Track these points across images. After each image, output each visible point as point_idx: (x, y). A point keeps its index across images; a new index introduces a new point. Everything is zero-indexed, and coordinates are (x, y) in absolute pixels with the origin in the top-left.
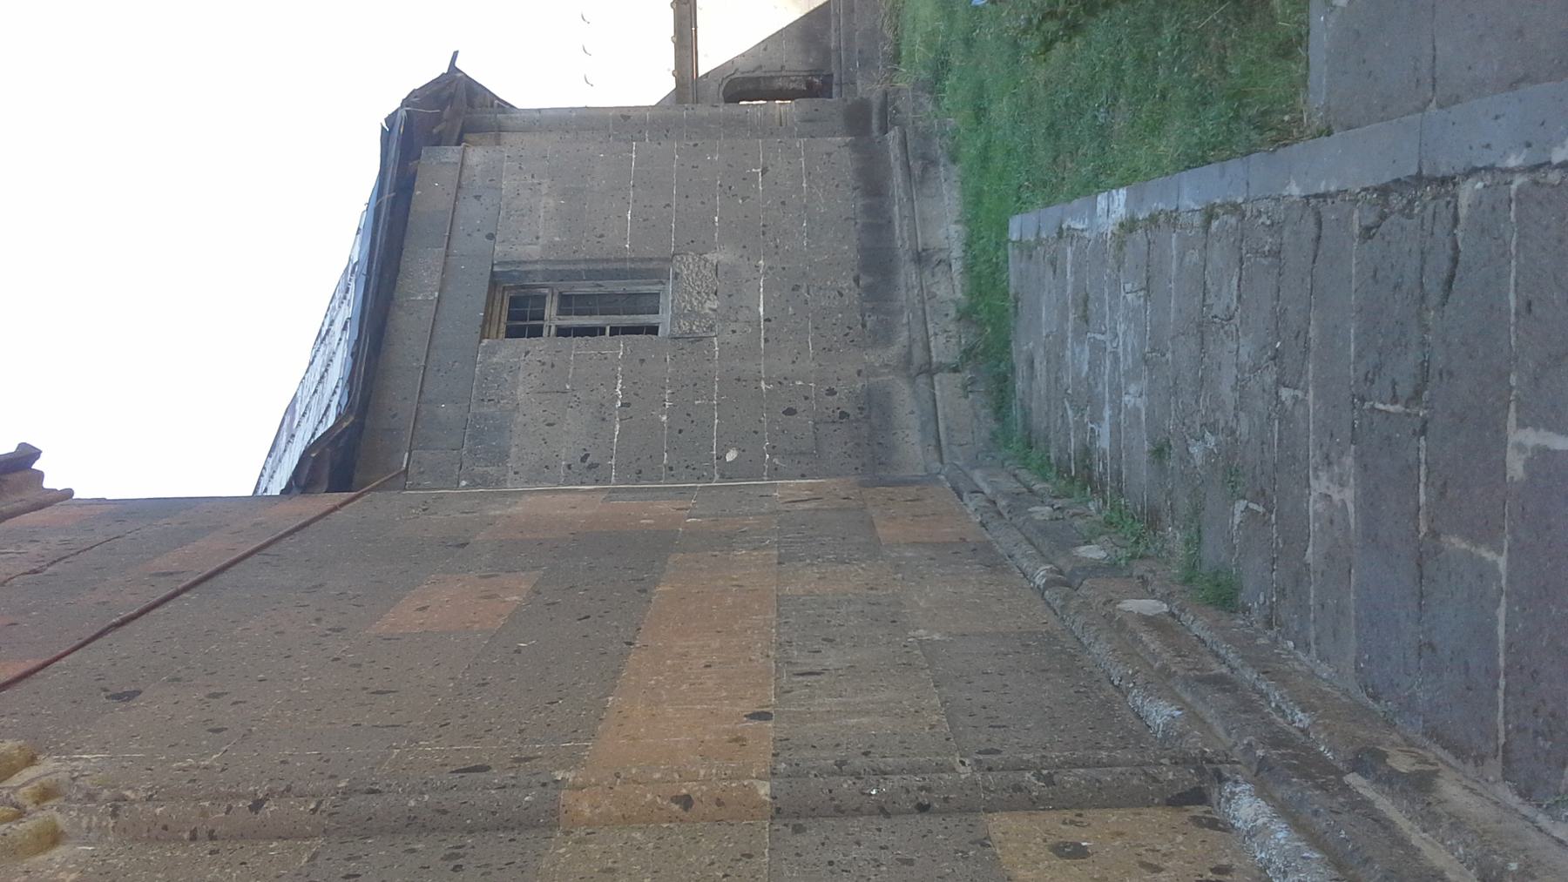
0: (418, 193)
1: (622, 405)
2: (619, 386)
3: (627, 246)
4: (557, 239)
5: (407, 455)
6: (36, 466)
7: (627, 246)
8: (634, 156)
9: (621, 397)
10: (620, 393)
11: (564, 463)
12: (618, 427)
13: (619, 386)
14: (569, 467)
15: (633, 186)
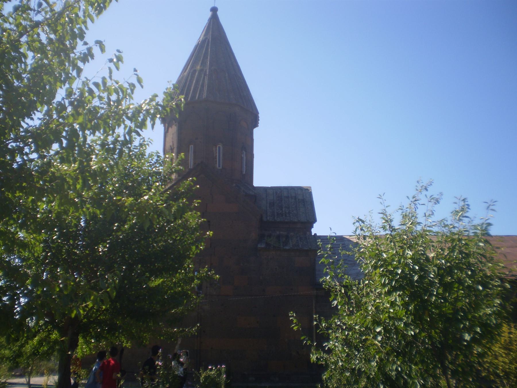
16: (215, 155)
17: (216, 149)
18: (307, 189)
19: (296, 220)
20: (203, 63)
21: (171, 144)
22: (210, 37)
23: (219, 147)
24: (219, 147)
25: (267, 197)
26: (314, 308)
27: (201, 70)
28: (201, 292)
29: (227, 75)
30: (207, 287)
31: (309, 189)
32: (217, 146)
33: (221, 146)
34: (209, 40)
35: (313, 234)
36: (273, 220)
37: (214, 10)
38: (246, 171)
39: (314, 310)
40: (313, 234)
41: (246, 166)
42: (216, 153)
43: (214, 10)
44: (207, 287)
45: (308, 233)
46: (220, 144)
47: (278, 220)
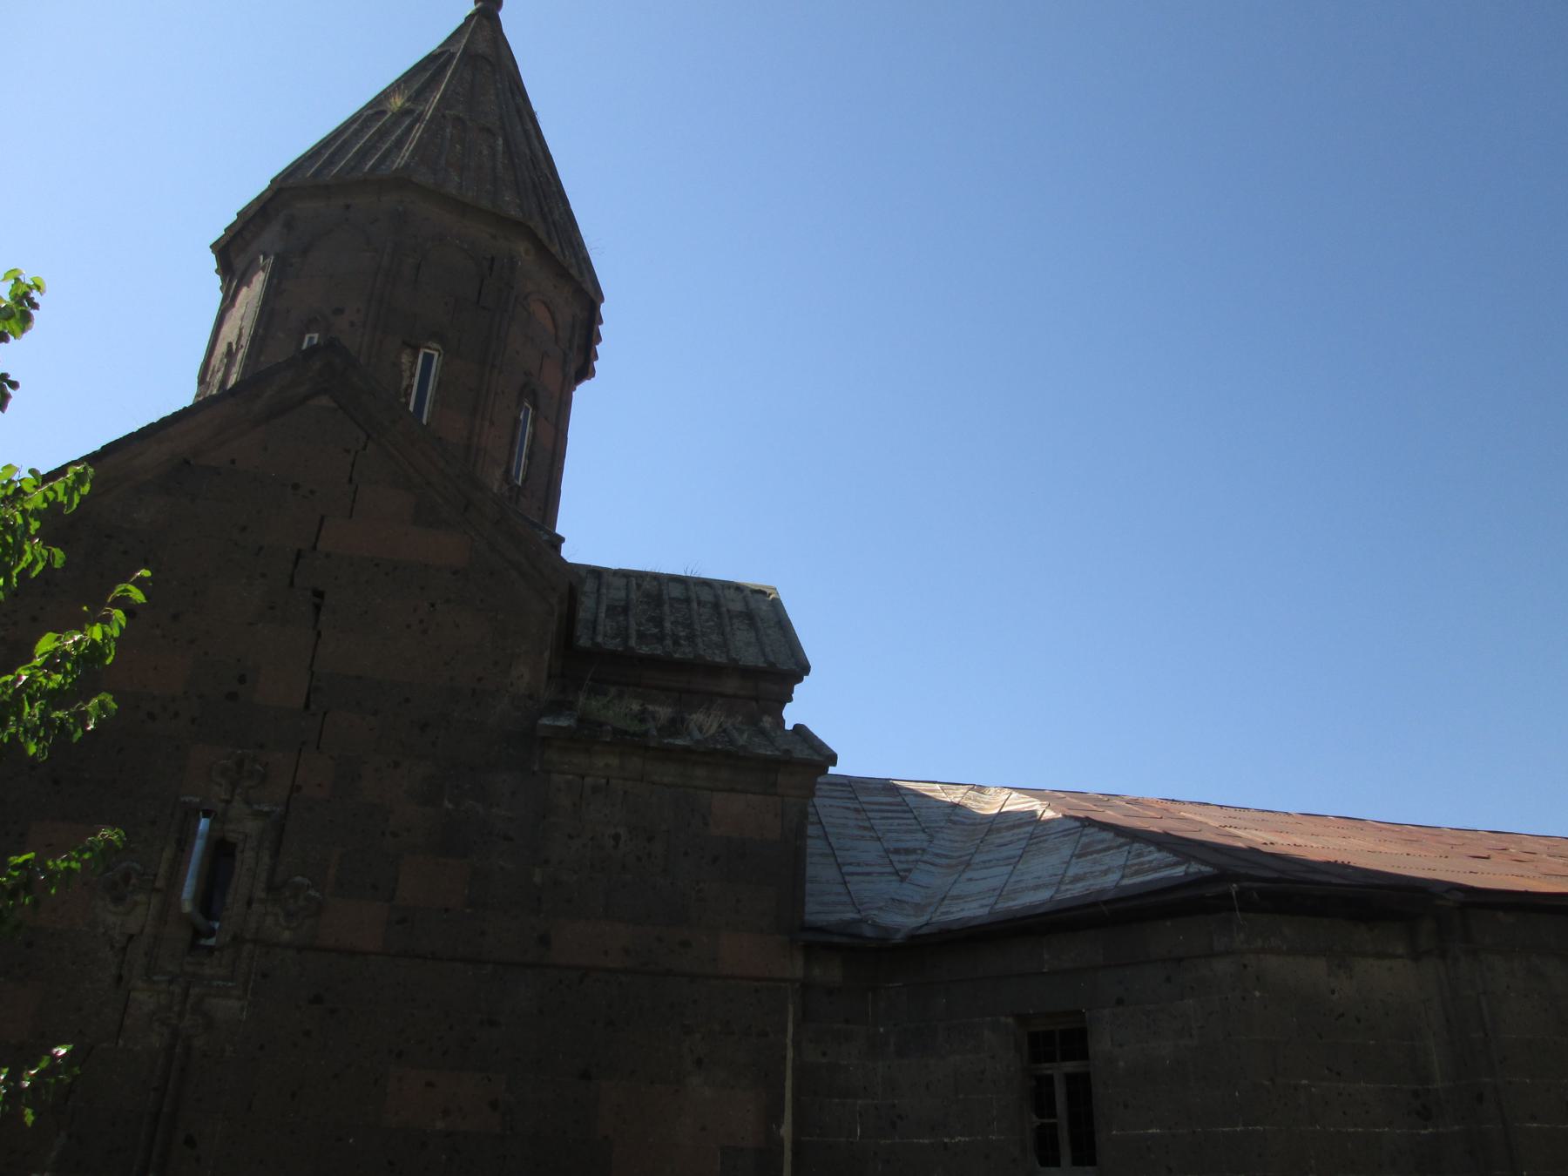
0: (1168, 923)
1: (946, 1143)
2: (963, 1139)
3: (1114, 1132)
4: (1121, 1064)
5: (900, 984)
7: (1114, 1132)
8: (1238, 1129)
9: (953, 1141)
10: (957, 1140)
11: (896, 1102)
12: (926, 1141)
13: (963, 1139)
14: (894, 1106)
15: (1194, 1132)
16: (405, 383)
17: (414, 363)
19: (720, 659)
20: (419, 96)
21: (233, 338)
22: (458, 49)
23: (428, 359)
24: (428, 359)
25: (598, 590)
26: (789, 1042)
27: (404, 112)
28: (217, 925)
29: (500, 141)
30: (249, 903)
31: (768, 591)
33: (436, 354)
34: (452, 55)
35: (789, 726)
36: (620, 649)
38: (524, 481)
39: (790, 1054)
40: (789, 726)
41: (530, 457)
42: (413, 375)
44: (249, 903)
45: (767, 721)
46: (435, 345)
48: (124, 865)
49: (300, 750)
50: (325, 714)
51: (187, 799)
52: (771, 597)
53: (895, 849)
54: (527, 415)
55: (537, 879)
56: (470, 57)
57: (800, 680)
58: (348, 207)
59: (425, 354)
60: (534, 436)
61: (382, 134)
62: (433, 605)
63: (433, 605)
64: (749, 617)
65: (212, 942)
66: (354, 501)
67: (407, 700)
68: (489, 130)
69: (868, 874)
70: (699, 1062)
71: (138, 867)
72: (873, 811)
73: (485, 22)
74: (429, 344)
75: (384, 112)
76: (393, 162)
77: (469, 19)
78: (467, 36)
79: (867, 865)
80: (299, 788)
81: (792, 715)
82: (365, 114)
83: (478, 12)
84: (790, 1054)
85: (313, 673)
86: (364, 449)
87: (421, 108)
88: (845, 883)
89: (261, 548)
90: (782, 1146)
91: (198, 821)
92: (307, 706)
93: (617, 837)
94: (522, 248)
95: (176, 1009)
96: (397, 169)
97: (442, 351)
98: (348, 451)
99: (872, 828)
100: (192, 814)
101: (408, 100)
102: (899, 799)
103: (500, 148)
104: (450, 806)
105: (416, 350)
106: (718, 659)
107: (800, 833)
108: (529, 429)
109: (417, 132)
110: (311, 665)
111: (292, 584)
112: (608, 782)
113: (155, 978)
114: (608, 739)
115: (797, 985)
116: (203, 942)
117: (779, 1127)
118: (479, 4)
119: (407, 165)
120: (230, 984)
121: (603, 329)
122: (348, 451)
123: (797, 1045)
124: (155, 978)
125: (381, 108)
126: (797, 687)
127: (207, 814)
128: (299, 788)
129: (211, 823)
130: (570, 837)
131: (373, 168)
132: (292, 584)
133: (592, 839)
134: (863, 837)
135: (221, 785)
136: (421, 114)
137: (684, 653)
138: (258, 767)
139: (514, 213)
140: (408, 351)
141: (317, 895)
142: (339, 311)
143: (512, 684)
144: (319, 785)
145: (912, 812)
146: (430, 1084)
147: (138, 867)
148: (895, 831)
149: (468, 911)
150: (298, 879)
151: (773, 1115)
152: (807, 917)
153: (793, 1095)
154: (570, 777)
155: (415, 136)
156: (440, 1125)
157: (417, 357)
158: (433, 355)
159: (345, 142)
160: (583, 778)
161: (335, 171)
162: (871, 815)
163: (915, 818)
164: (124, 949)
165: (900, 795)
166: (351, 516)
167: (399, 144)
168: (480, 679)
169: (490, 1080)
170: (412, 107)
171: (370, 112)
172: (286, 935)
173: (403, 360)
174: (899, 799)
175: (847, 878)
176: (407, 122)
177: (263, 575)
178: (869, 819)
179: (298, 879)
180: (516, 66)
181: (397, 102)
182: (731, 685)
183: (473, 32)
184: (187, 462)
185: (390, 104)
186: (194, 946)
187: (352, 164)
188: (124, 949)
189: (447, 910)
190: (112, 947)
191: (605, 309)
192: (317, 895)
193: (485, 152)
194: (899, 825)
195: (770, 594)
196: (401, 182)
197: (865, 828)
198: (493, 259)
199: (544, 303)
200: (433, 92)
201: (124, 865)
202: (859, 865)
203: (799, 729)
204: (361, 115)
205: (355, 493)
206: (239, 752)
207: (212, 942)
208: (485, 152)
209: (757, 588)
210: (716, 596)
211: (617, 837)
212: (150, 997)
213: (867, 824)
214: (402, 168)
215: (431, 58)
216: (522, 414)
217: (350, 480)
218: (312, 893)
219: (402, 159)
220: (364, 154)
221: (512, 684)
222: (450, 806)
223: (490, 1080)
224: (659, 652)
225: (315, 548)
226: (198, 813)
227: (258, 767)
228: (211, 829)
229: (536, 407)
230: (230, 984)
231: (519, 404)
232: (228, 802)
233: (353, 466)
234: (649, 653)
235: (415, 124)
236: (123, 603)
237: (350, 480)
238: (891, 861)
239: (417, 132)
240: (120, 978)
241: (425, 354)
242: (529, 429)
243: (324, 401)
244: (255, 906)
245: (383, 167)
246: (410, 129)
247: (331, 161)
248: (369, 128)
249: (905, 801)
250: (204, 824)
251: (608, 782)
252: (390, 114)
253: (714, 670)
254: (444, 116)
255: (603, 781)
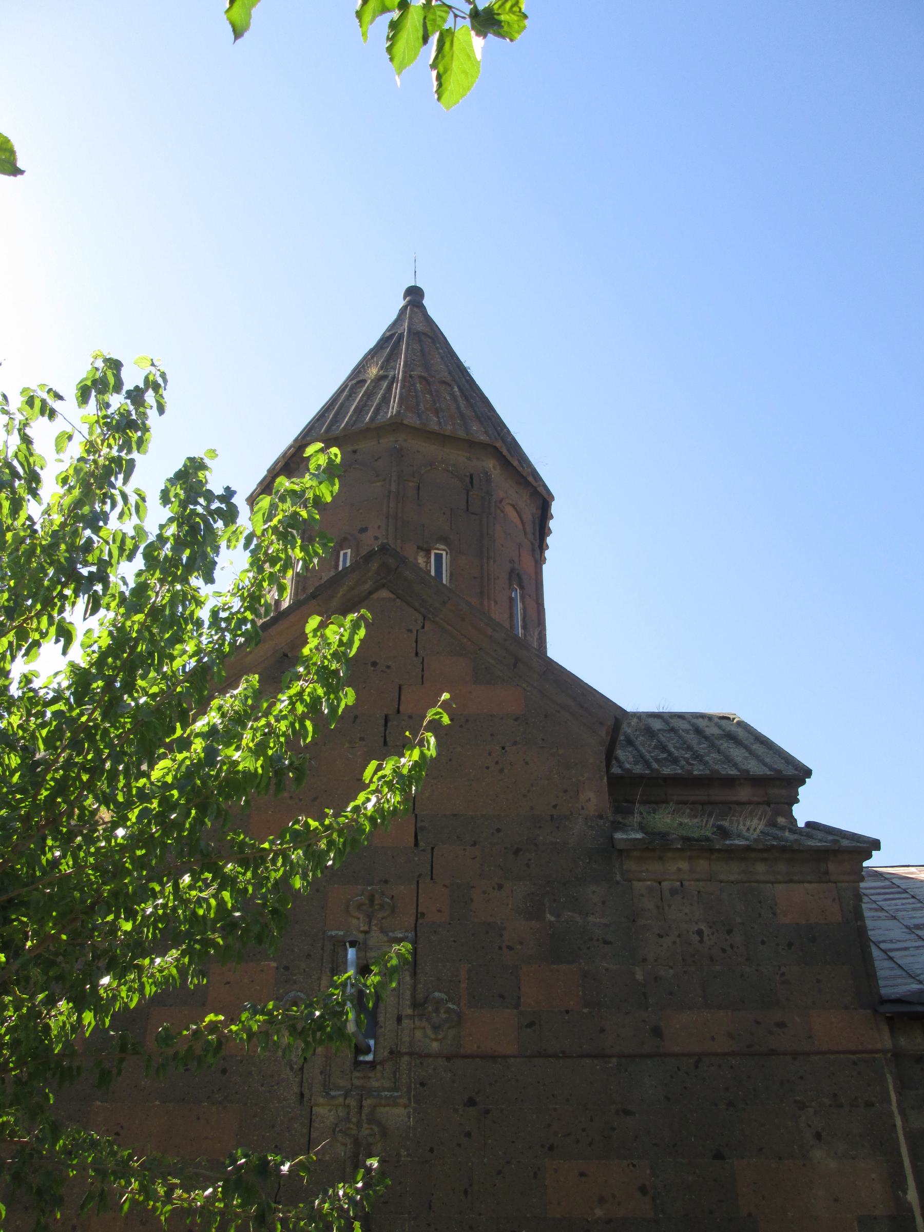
6: (874, 852)
17: (428, 562)
18: (728, 718)
23: (439, 557)
24: (439, 557)
27: (379, 379)
29: (456, 389)
30: (399, 1020)
31: (731, 717)
32: (430, 554)
33: (444, 553)
34: (401, 336)
37: (414, 295)
39: (899, 1123)
43: (414, 295)
44: (399, 1020)
47: (667, 771)
48: (292, 994)
49: (418, 882)
50: (433, 848)
51: (333, 933)
52: (735, 721)
53: (915, 925)
54: (517, 594)
55: (639, 976)
56: (414, 334)
57: (803, 782)
58: (355, 452)
59: (436, 554)
60: (524, 609)
61: (369, 395)
62: (503, 748)
63: (503, 748)
64: (731, 737)
65: (370, 1058)
66: (423, 670)
67: (499, 830)
68: (444, 382)
69: (906, 949)
70: (818, 1136)
71: (302, 996)
72: (872, 895)
73: (415, 309)
74: (438, 546)
75: (364, 381)
76: (387, 413)
77: (403, 311)
78: (407, 321)
79: (899, 941)
80: (423, 915)
81: (802, 814)
82: (350, 384)
83: (409, 303)
84: (899, 1123)
85: (416, 815)
86: (423, 627)
87: (392, 373)
88: (891, 958)
89: (356, 717)
90: (911, 1209)
91: (346, 950)
92: (416, 844)
93: (700, 933)
94: (491, 465)
95: (354, 1120)
96: (391, 416)
97: (448, 551)
98: (410, 631)
99: (882, 909)
100: (340, 945)
101: (382, 368)
102: (887, 883)
103: (458, 393)
104: (553, 919)
105: (428, 552)
106: (731, 773)
107: (858, 914)
108: (520, 605)
109: (397, 390)
110: (414, 809)
111: (385, 743)
112: (682, 885)
113: (333, 1093)
114: (679, 847)
115: (889, 1055)
116: (361, 1058)
117: (905, 1193)
118: (408, 299)
119: (398, 412)
120: (396, 1094)
121: (552, 524)
122: (410, 631)
123: (902, 1113)
124: (333, 1093)
125: (361, 378)
126: (801, 790)
127: (353, 944)
128: (423, 915)
129: (357, 952)
130: (660, 936)
131: (373, 419)
132: (385, 743)
133: (679, 936)
134: (880, 917)
135: (358, 919)
136: (394, 377)
137: (698, 770)
138: (387, 900)
139: (483, 438)
140: (422, 553)
141: (455, 1007)
142: (363, 530)
143: (583, 808)
144: (439, 911)
145: (907, 892)
146: (582, 1174)
147: (302, 996)
148: (904, 910)
149: (585, 1011)
150: (437, 994)
151: (898, 1182)
152: (883, 991)
153: (911, 1162)
154: (649, 883)
155: (396, 393)
156: (599, 1212)
157: (430, 557)
158: (442, 554)
159: (342, 405)
160: (660, 883)
161: (343, 425)
162: (873, 898)
163: (913, 897)
164: (302, 1069)
165: (886, 879)
166: (423, 683)
167: (386, 399)
168: (555, 806)
169: (634, 1166)
170: (385, 373)
171: (354, 382)
172: (435, 1046)
173: (419, 561)
174: (887, 883)
175: (891, 954)
176: (385, 384)
177: (362, 739)
178: (875, 902)
179: (437, 994)
180: (445, 338)
181: (373, 371)
182: (744, 793)
183: (410, 318)
184: (287, 656)
185: (368, 373)
186: (357, 1064)
187: (354, 419)
188: (302, 1069)
189: (567, 1012)
190: (292, 1068)
191: (555, 508)
192: (455, 1007)
193: (448, 398)
194: (903, 904)
195: (734, 719)
196: (396, 425)
197: (876, 910)
198: (471, 477)
199: (513, 506)
200: (396, 361)
201: (292, 994)
202: (891, 941)
203: (808, 824)
204: (346, 386)
205: (422, 663)
206: (369, 888)
207: (370, 1058)
208: (448, 398)
209: (721, 715)
210: (693, 725)
211: (700, 933)
212: (330, 1111)
213: (874, 906)
214: (395, 415)
215: (384, 341)
216: (513, 593)
217: (417, 654)
218: (450, 1005)
219: (393, 408)
220: (360, 410)
221: (583, 808)
222: (553, 919)
223: (634, 1166)
224: (680, 771)
225: (398, 711)
226: (345, 945)
227: (387, 900)
228: (358, 958)
229: (522, 587)
230: (396, 1094)
231: (510, 585)
232: (366, 932)
233: (416, 642)
234: (672, 773)
235: (392, 384)
236: (435, 726)
237: (417, 654)
238: (917, 935)
239: (396, 389)
240: (302, 1095)
241: (436, 554)
242: (520, 605)
243: (384, 594)
244: (406, 1022)
245: (379, 417)
246: (389, 388)
247: (335, 421)
248: (357, 393)
249: (894, 884)
250: (351, 953)
251: (682, 885)
252: (369, 382)
253: (729, 782)
254: (411, 376)
255: (678, 883)
